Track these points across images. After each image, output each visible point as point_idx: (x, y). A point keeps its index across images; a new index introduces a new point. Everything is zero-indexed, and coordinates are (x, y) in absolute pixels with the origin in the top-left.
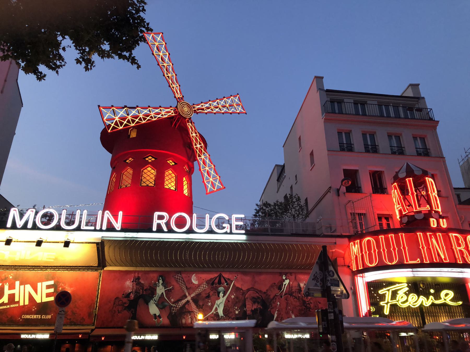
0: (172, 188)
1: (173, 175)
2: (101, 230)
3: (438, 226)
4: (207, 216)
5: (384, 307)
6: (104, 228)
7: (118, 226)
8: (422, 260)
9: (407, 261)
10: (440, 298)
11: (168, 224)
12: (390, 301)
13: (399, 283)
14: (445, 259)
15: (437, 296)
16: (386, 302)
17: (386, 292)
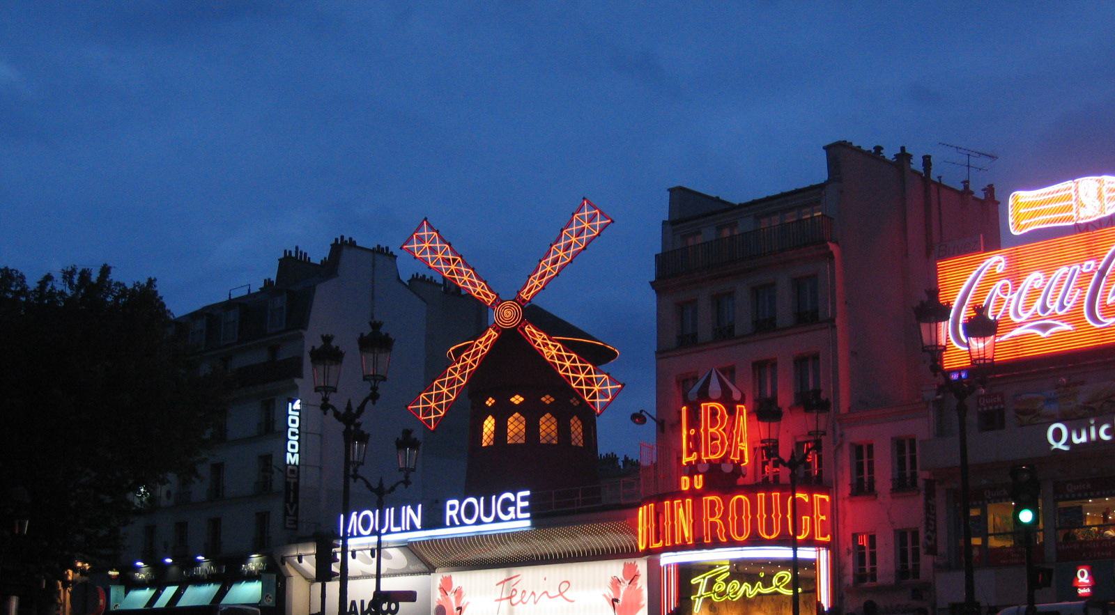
0: (521, 441)
1: (522, 418)
2: (406, 531)
3: (689, 489)
4: (494, 497)
5: (695, 601)
6: (408, 528)
7: (418, 523)
8: (664, 540)
9: (652, 545)
10: (772, 585)
11: (458, 515)
12: (703, 594)
13: (720, 566)
14: (689, 539)
15: (767, 583)
16: (698, 595)
17: (700, 581)
